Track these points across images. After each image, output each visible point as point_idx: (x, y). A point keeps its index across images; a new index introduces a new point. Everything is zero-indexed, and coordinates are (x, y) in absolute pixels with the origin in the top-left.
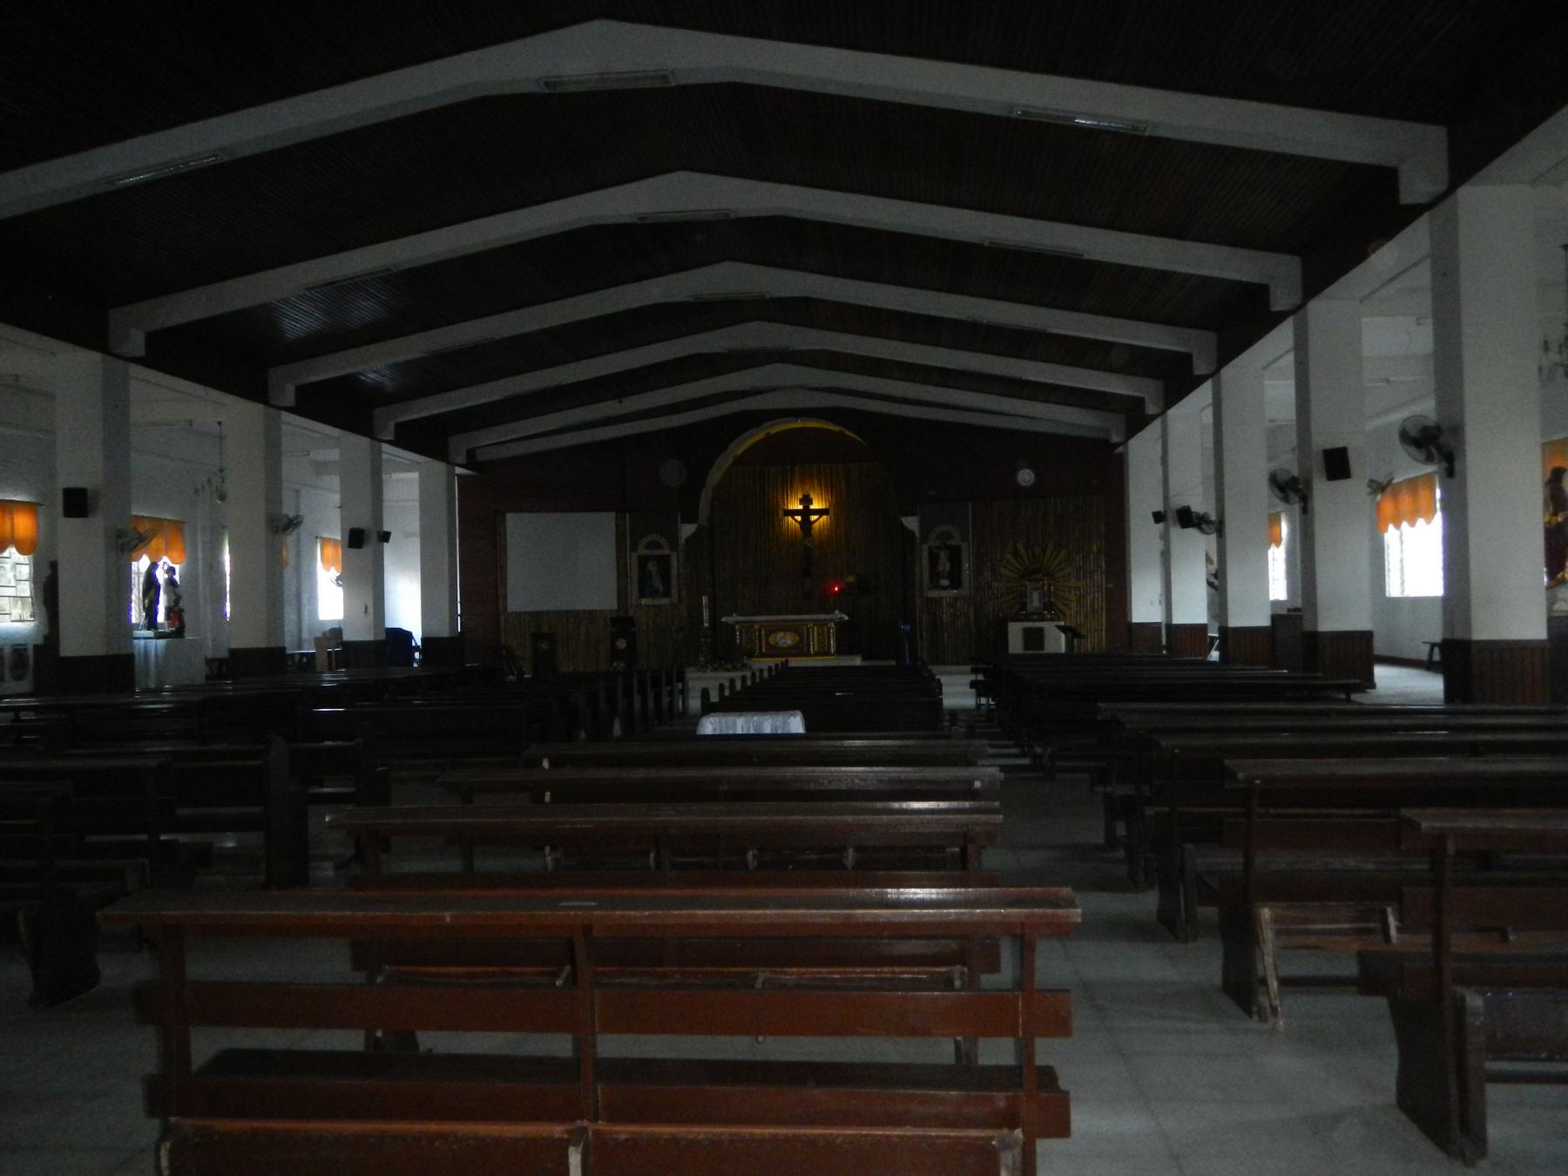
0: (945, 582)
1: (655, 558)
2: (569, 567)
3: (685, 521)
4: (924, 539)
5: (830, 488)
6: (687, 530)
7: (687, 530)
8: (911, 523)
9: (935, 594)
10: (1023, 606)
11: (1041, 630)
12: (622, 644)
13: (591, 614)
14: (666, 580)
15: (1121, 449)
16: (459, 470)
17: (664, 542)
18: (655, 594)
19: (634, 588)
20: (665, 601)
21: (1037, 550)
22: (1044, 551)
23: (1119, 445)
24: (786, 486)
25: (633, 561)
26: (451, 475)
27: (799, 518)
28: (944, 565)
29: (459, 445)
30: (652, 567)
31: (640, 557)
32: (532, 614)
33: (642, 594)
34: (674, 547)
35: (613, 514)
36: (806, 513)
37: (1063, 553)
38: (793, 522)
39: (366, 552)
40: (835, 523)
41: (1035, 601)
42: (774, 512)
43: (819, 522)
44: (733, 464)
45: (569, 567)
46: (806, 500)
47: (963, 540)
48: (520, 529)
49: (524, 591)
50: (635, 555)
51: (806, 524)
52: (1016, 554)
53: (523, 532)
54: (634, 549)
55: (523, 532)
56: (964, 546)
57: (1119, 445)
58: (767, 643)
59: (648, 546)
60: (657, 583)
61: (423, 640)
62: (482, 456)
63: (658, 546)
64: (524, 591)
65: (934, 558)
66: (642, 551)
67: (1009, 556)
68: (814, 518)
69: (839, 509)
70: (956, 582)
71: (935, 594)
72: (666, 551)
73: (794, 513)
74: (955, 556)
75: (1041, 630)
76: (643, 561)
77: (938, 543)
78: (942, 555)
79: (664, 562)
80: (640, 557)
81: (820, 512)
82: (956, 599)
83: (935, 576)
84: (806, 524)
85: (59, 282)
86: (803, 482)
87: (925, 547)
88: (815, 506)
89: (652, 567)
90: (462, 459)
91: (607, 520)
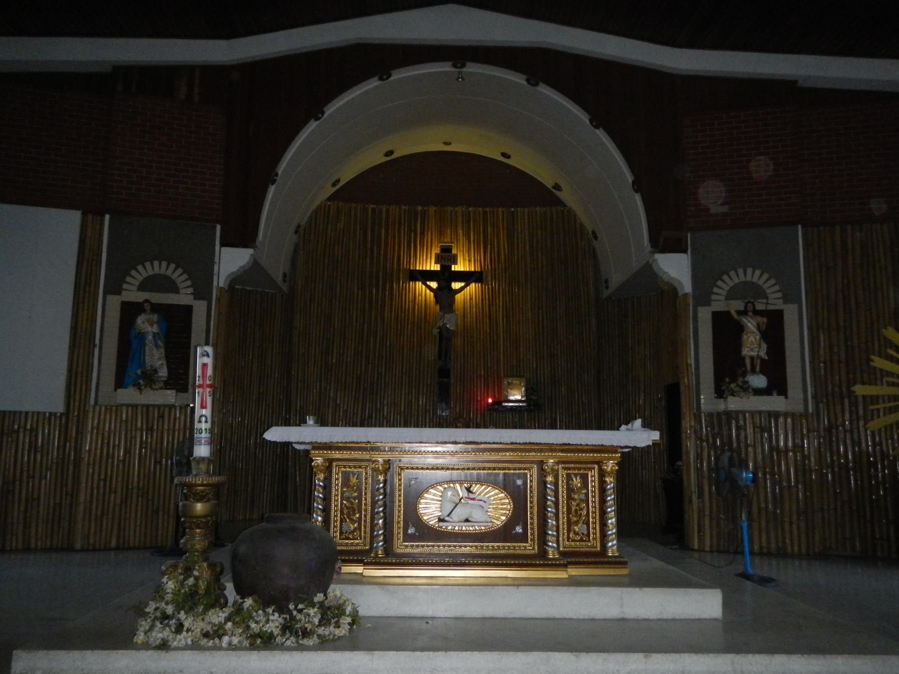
0: (759, 381)
1: (157, 308)
4: (702, 295)
6: (231, 261)
7: (231, 261)
8: (676, 268)
9: (733, 404)
18: (149, 379)
24: (414, 242)
25: (108, 313)
27: (434, 285)
30: (147, 325)
33: (120, 383)
34: (202, 290)
35: (75, 217)
36: (446, 276)
38: (424, 291)
43: (466, 293)
44: (329, 199)
46: (446, 257)
47: (787, 299)
50: (114, 302)
51: (445, 295)
54: (114, 288)
58: (412, 516)
59: (142, 287)
60: (155, 358)
63: (173, 288)
65: (727, 330)
68: (456, 285)
71: (733, 404)
72: (184, 298)
73: (426, 276)
74: (773, 330)
76: (130, 311)
77: (736, 306)
78: (750, 324)
83: (729, 370)
84: (445, 295)
87: (705, 315)
89: (147, 325)
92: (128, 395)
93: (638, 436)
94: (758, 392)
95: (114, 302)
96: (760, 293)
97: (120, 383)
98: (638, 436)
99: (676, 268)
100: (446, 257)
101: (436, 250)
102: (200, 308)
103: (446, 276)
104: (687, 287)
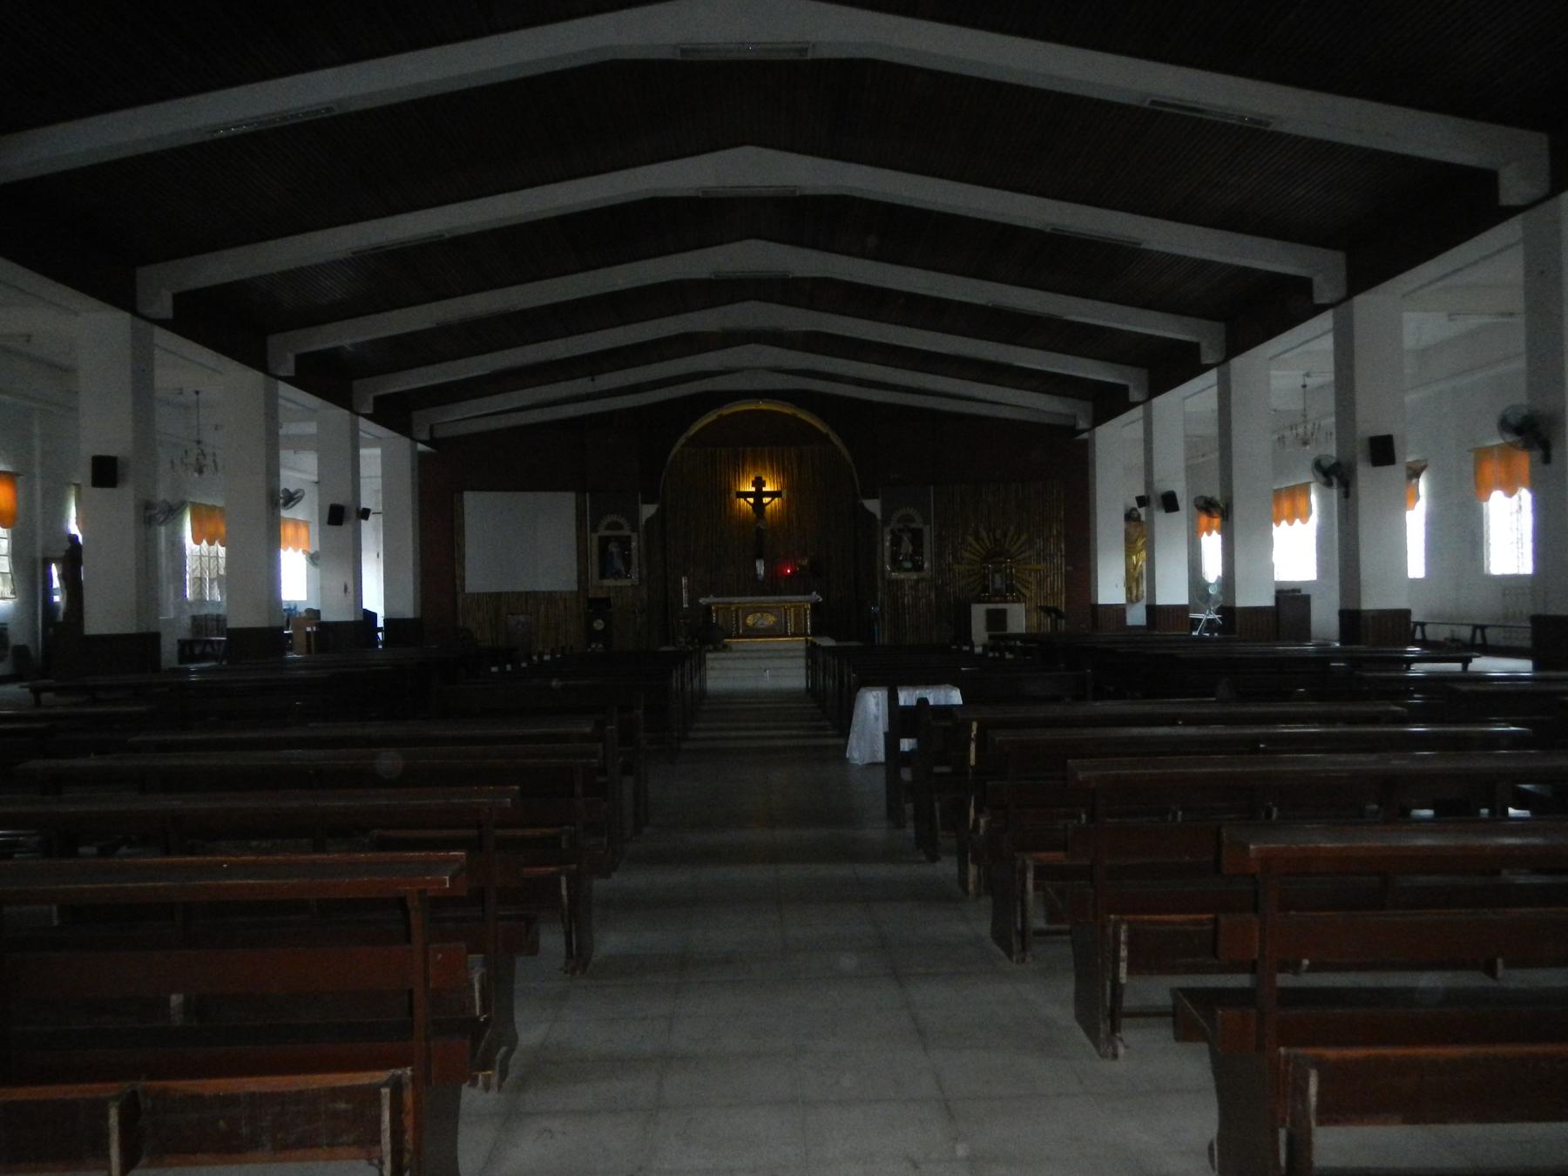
0: (908, 565)
1: (618, 539)
2: (528, 548)
3: (646, 502)
5: (782, 470)
6: (648, 511)
7: (648, 511)
8: (873, 506)
10: (985, 589)
11: (1004, 612)
12: (599, 625)
13: (550, 597)
14: (627, 561)
15: (1085, 436)
16: (421, 447)
17: (622, 521)
18: (617, 575)
19: (594, 570)
20: (626, 582)
21: (998, 534)
22: (1005, 535)
23: (1083, 431)
24: (737, 469)
25: (593, 541)
26: (414, 448)
27: (751, 500)
28: (907, 547)
29: (423, 420)
30: (613, 548)
31: (600, 538)
32: (490, 595)
33: (603, 576)
34: (634, 528)
36: (759, 495)
37: (1024, 537)
38: (746, 504)
39: (347, 528)
40: (788, 503)
41: (998, 582)
42: (723, 493)
45: (528, 548)
46: (759, 483)
48: (479, 509)
49: (481, 573)
51: (759, 506)
52: (978, 538)
53: (481, 511)
54: (594, 529)
55: (481, 511)
56: (926, 530)
57: (1083, 431)
58: (745, 624)
59: (608, 527)
60: (619, 564)
61: (386, 621)
62: (439, 434)
63: (620, 527)
64: (481, 573)
65: (896, 542)
66: (603, 532)
67: (970, 539)
68: (766, 500)
69: (794, 491)
70: (918, 568)
72: (626, 532)
73: (746, 495)
74: (917, 537)
75: (1004, 612)
76: (604, 542)
79: (624, 543)
80: (600, 538)
81: (772, 495)
82: (917, 581)
84: (759, 506)
85: (89, 238)
86: (755, 465)
88: (767, 488)
90: (425, 436)
91: (568, 500)
92: (608, 582)
93: (815, 596)
94: (907, 570)
95: (595, 537)
96: (913, 520)
97: (603, 576)
98: (815, 596)
99: (873, 506)
100: (759, 483)
101: (752, 478)
102: (634, 536)
103: (759, 495)
104: (879, 516)
